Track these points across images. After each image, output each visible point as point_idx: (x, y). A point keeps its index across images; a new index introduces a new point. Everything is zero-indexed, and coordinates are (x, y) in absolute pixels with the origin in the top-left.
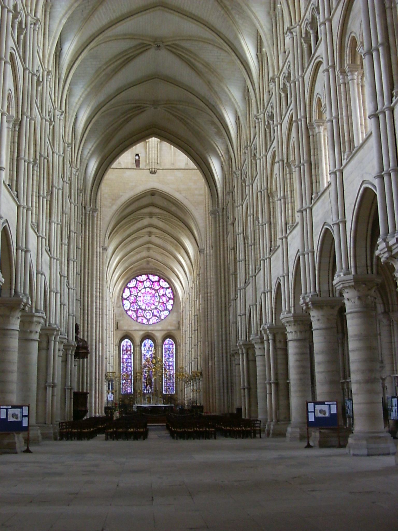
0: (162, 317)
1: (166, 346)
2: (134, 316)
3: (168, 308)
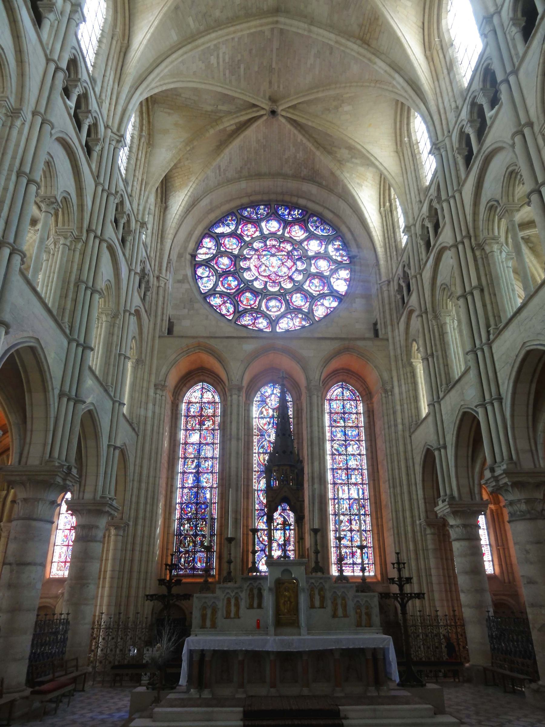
0: (320, 312)
1: (334, 404)
2: (227, 309)
3: (335, 287)
